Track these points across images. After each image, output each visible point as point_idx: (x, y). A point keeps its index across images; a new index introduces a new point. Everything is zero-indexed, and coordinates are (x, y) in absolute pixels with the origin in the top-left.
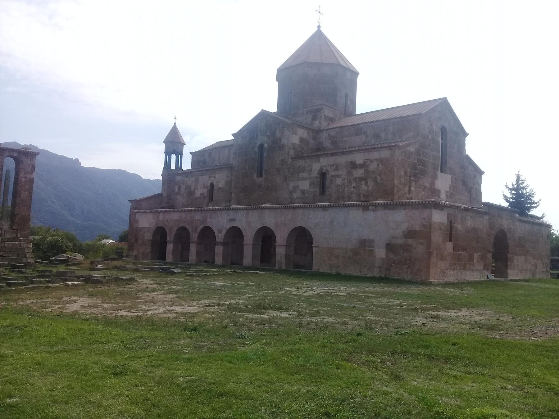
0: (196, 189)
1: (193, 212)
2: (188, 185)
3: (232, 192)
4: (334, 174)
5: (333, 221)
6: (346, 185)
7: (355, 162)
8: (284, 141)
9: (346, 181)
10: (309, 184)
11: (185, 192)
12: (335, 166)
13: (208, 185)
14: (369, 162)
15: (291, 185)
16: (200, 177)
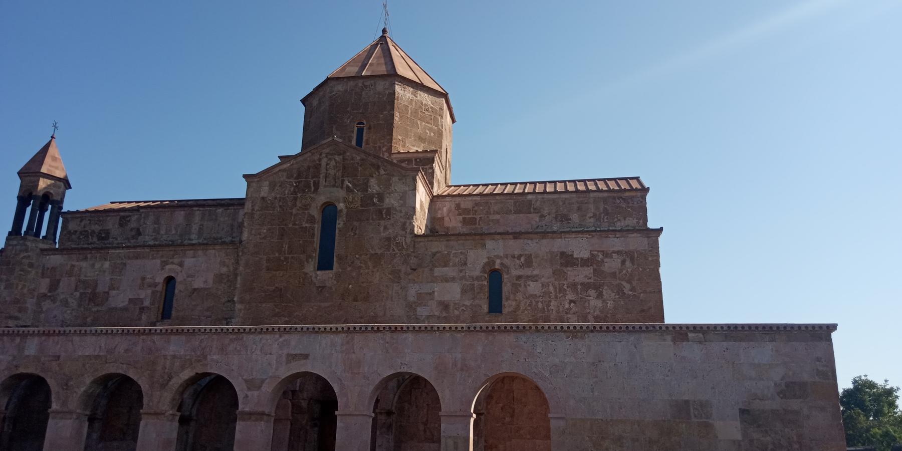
0: (112, 288)
1: (155, 338)
2: (87, 278)
3: (235, 299)
4: (521, 273)
5: (600, 362)
6: (553, 295)
7: (570, 253)
8: (391, 201)
9: (551, 288)
10: (459, 290)
11: (72, 294)
12: (522, 259)
13: (156, 281)
14: (601, 256)
15: (412, 292)
16: (129, 261)
